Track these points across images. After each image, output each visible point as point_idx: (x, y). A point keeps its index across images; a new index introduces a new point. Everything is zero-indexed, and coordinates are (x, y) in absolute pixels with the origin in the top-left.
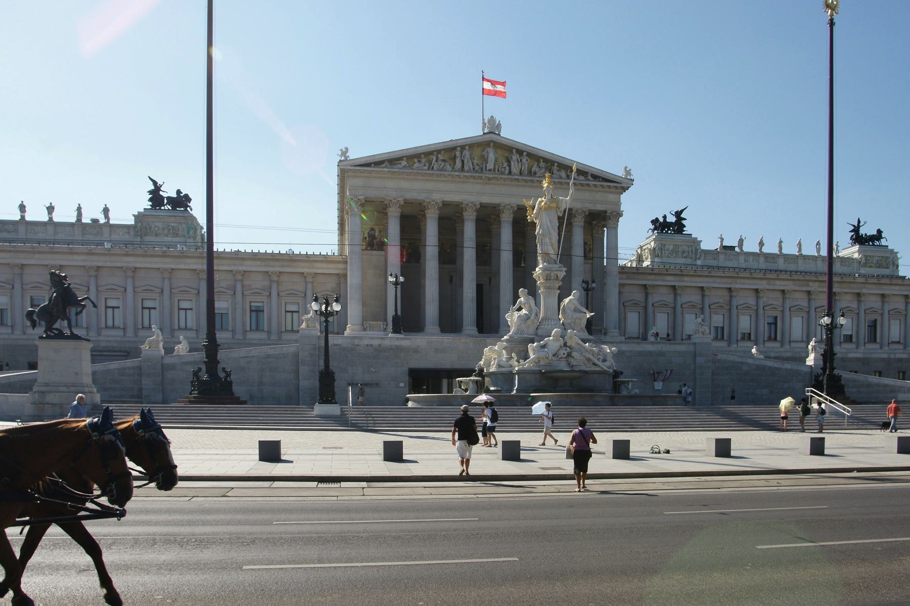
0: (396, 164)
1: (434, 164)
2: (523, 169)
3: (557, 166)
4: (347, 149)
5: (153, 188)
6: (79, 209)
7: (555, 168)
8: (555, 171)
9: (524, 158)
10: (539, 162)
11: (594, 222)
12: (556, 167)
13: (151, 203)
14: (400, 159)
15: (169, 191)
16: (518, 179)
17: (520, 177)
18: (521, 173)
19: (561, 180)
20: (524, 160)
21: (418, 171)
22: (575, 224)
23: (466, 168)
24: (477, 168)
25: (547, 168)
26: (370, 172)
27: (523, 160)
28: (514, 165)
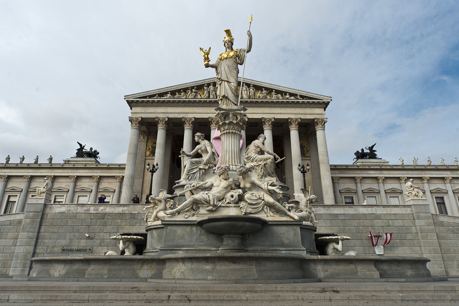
0: (165, 96)
1: (190, 95)
2: (250, 95)
3: (275, 92)
5: (79, 147)
8: (274, 96)
9: (251, 89)
10: (262, 91)
12: (274, 93)
13: (76, 155)
14: (166, 93)
15: (87, 149)
16: (248, 101)
17: (248, 100)
20: (251, 90)
21: (177, 99)
22: (292, 129)
23: (211, 96)
28: (244, 93)
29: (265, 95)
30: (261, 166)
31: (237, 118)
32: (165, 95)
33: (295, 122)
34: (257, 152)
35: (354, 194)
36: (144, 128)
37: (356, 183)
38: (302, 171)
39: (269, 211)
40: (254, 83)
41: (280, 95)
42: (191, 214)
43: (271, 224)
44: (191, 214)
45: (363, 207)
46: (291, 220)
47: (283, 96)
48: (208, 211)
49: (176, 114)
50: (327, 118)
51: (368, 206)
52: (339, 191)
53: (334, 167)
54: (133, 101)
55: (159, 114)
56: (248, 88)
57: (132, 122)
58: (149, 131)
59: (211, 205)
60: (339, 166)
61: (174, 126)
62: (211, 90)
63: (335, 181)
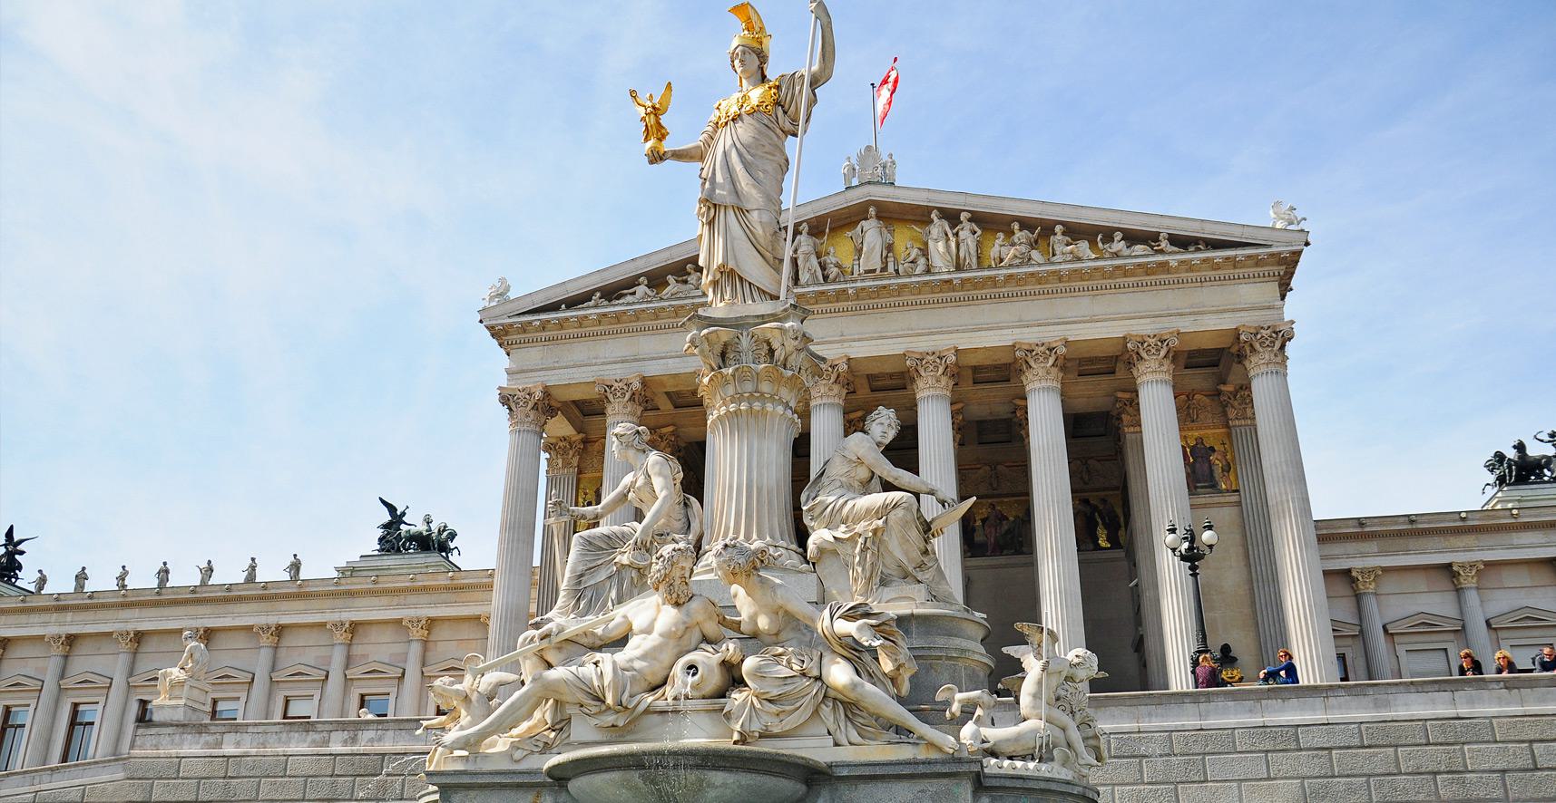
0: (626, 295)
3: (1064, 234)
4: (502, 280)
6: (253, 568)
7: (1058, 238)
10: (1011, 233)
11: (1228, 388)
12: (1059, 237)
14: (631, 283)
18: (959, 268)
19: (1078, 265)
21: (673, 303)
22: (1144, 378)
23: (804, 277)
24: (833, 271)
25: (1036, 242)
26: (561, 324)
27: (961, 233)
29: (1023, 248)
30: (861, 540)
31: (771, 352)
32: (625, 291)
33: (1153, 351)
34: (856, 484)
35: (1451, 636)
36: (560, 427)
37: (1457, 590)
38: (1183, 552)
39: (842, 725)
40: (977, 206)
41: (1084, 246)
42: (538, 743)
43: (847, 776)
44: (538, 743)
45: (1412, 689)
46: (933, 755)
47: (1100, 245)
48: (599, 728)
49: (670, 361)
50: (1293, 322)
51: (1437, 687)
52: (1384, 627)
53: (1354, 527)
54: (511, 325)
55: (609, 367)
56: (952, 227)
57: (510, 409)
58: (581, 436)
59: (609, 708)
60: (1376, 520)
61: (676, 407)
62: (807, 254)
63: (1361, 587)
